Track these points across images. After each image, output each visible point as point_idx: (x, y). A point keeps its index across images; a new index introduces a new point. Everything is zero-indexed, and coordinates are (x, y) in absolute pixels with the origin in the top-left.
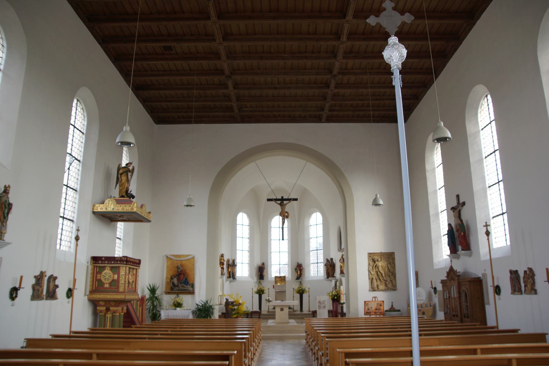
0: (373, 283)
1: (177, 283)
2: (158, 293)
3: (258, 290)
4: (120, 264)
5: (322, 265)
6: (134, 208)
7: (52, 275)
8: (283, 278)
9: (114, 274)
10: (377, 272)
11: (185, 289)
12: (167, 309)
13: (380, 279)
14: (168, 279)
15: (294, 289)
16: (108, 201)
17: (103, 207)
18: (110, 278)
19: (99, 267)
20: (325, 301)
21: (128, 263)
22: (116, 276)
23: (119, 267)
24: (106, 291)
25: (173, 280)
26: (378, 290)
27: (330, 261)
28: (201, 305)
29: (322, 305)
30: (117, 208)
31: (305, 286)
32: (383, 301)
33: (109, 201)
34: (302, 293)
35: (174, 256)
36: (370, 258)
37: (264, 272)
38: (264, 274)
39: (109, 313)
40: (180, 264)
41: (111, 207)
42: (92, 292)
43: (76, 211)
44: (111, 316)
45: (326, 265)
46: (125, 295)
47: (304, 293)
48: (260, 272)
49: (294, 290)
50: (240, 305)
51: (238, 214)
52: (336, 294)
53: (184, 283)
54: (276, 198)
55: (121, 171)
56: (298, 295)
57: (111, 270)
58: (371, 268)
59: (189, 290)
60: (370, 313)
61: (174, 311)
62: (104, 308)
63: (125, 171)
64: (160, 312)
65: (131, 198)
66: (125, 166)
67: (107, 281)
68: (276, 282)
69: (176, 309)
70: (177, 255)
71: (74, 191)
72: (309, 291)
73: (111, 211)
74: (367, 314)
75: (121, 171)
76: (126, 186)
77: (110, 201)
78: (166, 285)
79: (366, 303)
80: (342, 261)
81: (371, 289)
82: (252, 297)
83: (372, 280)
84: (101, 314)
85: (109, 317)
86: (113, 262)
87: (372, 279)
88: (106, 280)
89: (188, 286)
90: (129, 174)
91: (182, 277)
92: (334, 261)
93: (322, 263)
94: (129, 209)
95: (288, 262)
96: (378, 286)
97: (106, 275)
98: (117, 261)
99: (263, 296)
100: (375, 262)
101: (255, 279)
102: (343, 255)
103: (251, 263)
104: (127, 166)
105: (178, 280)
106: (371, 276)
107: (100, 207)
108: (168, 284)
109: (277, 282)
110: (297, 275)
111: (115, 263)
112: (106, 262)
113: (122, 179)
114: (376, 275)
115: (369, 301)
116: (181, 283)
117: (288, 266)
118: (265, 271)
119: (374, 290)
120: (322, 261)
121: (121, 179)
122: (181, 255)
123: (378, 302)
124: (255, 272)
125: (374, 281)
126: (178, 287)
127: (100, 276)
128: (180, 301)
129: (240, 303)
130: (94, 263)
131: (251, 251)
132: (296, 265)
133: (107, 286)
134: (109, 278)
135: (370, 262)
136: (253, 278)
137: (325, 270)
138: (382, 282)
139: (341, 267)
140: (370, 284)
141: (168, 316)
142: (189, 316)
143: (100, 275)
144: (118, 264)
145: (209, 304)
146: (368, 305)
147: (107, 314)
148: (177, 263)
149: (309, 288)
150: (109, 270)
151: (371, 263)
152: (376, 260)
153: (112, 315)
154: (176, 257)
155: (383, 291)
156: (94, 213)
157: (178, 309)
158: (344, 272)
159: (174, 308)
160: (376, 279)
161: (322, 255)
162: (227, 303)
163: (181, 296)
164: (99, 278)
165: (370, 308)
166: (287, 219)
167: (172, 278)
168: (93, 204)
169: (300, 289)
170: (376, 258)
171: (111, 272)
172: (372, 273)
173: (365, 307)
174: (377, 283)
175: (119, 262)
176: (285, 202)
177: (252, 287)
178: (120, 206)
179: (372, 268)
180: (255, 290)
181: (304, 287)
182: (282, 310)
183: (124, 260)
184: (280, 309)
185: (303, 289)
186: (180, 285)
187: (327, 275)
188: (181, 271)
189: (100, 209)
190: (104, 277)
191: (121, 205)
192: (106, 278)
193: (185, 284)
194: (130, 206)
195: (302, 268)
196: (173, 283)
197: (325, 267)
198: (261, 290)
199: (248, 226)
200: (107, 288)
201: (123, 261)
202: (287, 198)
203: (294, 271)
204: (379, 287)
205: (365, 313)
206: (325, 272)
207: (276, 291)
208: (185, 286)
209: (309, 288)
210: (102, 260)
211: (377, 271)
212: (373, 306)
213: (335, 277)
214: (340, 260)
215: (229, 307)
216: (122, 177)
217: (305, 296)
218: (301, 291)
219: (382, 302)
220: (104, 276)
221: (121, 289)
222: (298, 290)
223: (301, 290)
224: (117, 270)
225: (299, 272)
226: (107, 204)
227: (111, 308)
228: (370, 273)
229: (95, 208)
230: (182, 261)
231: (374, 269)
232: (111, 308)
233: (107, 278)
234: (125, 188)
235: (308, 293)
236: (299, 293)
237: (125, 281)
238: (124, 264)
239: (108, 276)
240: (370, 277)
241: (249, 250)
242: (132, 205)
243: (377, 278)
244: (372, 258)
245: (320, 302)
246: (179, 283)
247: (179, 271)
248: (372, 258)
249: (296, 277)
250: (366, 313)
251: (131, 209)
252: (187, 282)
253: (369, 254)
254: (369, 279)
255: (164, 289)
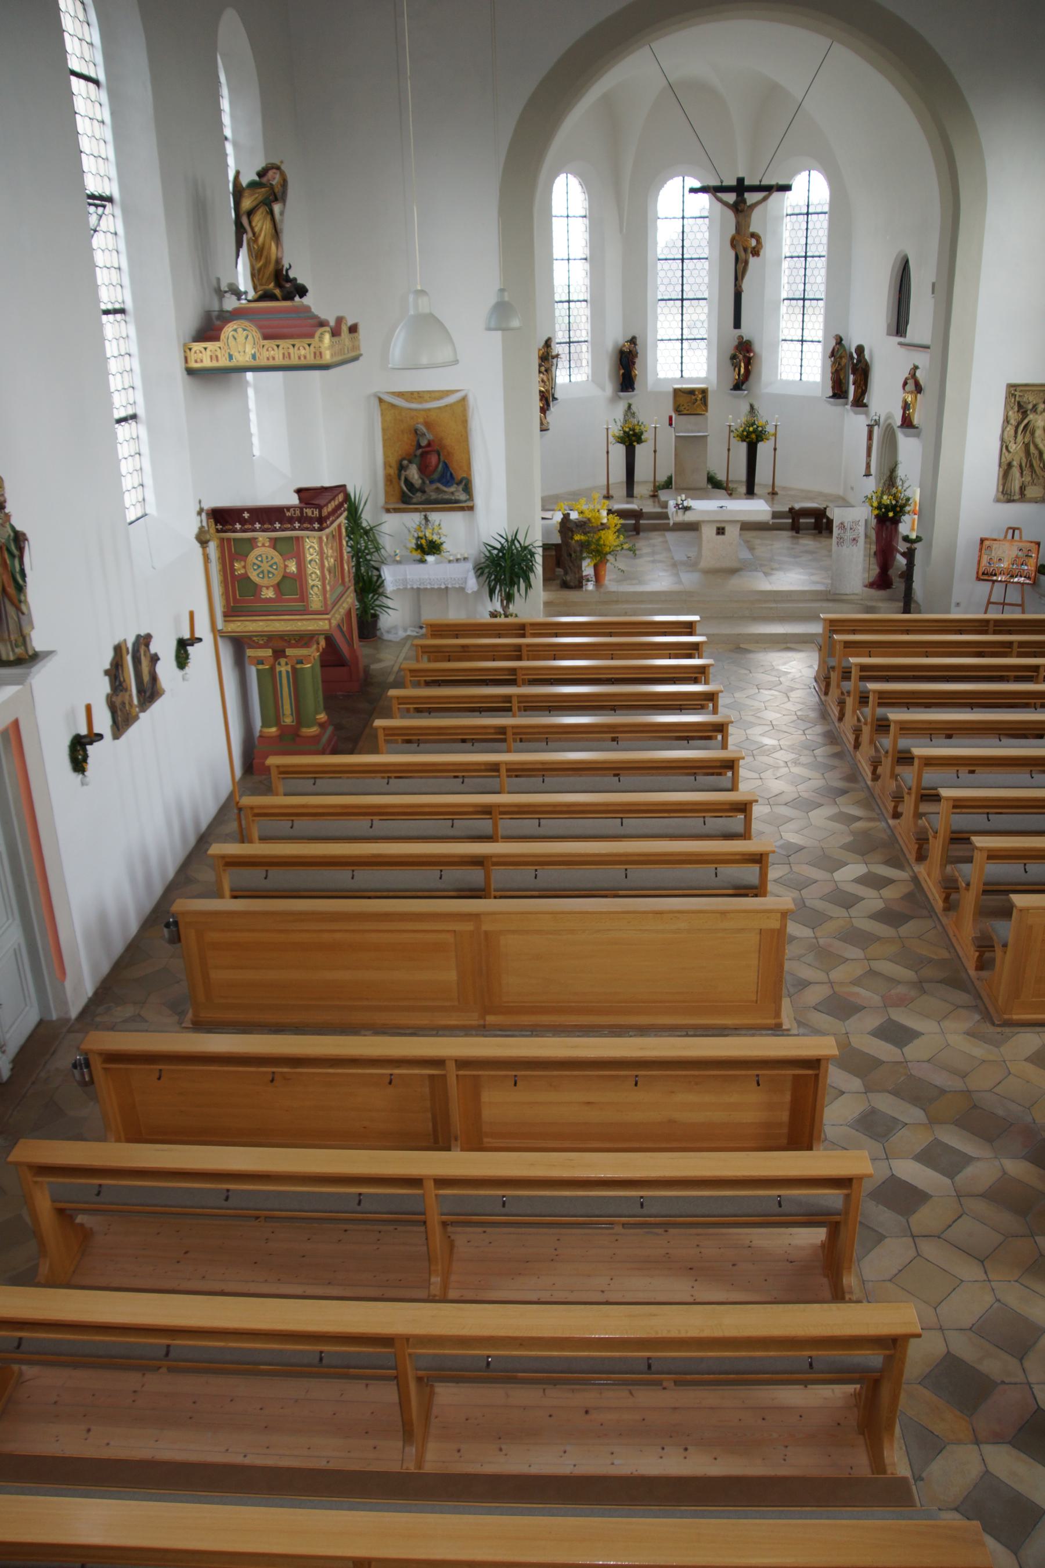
0: (1010, 478)
1: (420, 481)
2: (367, 518)
3: (625, 432)
4: (300, 529)
5: (819, 347)
6: (322, 350)
7: (138, 637)
8: (700, 396)
9: (285, 557)
10: (1027, 446)
11: (446, 497)
12: (399, 562)
13: (1031, 466)
14: (390, 467)
15: (732, 428)
16: (230, 329)
17: (219, 353)
18: (276, 569)
19: (234, 539)
20: (857, 523)
21: (325, 525)
22: (293, 568)
23: (297, 538)
24: (267, 611)
25: (407, 473)
26: (1023, 497)
27: (855, 356)
28: (499, 546)
29: (849, 535)
30: (265, 354)
31: (768, 418)
32: (1038, 544)
33: (235, 330)
34: (755, 440)
35: (400, 395)
36: (1013, 400)
37: (636, 366)
38: (637, 371)
39: (283, 661)
40: (421, 420)
41: (244, 352)
42: (230, 613)
43: (138, 383)
44: (290, 670)
45: (833, 354)
46: (329, 620)
47: (762, 440)
48: (623, 368)
49: (731, 431)
50: (602, 530)
51: (553, 182)
52: (894, 502)
53: (439, 480)
54: (719, 184)
55: (247, 204)
56: (743, 447)
57: (274, 548)
58: (1010, 430)
59: (457, 502)
60: (995, 575)
61: (421, 566)
62: (269, 652)
63: (261, 198)
64: (378, 569)
65: (297, 298)
66: (257, 178)
67: (266, 579)
68: (679, 406)
69: (422, 561)
70: (412, 393)
71: (119, 316)
72: (775, 435)
73: (247, 364)
74: (986, 577)
75: (247, 204)
76: (273, 257)
77: (240, 330)
78: (386, 485)
79: (986, 543)
80: (911, 386)
81: (1002, 497)
82: (608, 452)
83: (1006, 470)
84: (260, 667)
85: (284, 675)
86: (277, 525)
87: (1010, 465)
88: (263, 578)
89: (452, 489)
90: (277, 208)
91: (433, 459)
92: (867, 357)
93: (819, 342)
94: (308, 357)
95: (709, 331)
96: (1022, 489)
97: (262, 561)
98: (291, 520)
99: (639, 449)
100: (1025, 414)
101: (609, 388)
102: (916, 368)
103: (596, 341)
104: (264, 180)
105: (423, 470)
106: (1008, 457)
107: (209, 353)
108: (391, 481)
109: (682, 408)
110: (737, 377)
111: (285, 526)
112: (258, 526)
113: (257, 229)
114: (1023, 455)
115: (995, 540)
116: (431, 482)
117: (709, 346)
118: (638, 361)
119: (1009, 501)
120: (819, 335)
121: (254, 234)
122: (423, 392)
123: (1021, 545)
124: (607, 366)
125: (1015, 471)
126: (424, 492)
127: (244, 567)
128: (435, 538)
129: (602, 524)
130: (218, 531)
131: (596, 301)
132: (736, 343)
133: (270, 594)
134: (273, 571)
135: (1010, 413)
136: (603, 389)
137: (829, 370)
138: (1037, 475)
139: (906, 406)
140: (1001, 482)
141: (405, 581)
142: (465, 580)
143: (243, 563)
144: (294, 529)
145: (522, 543)
146: (992, 551)
147: (277, 663)
148: (412, 418)
149: (776, 426)
150: (269, 547)
151: (1014, 416)
152: (1030, 406)
153: (294, 669)
154: (407, 400)
155: (1036, 502)
156: (190, 372)
157: (430, 559)
158: (915, 422)
159: (417, 555)
160: (1021, 466)
161: (821, 318)
162: (566, 526)
163: (435, 517)
164: (243, 571)
165: (995, 560)
166: (755, 257)
167: (401, 468)
168: (182, 342)
169: (751, 429)
170: (1031, 399)
171: (276, 553)
172: (1013, 447)
173: (980, 556)
174: (1023, 479)
175: (297, 525)
176: (751, 198)
177: (608, 424)
178: (275, 348)
179: (1012, 432)
180: (616, 430)
181: (761, 422)
182: (721, 531)
183: (311, 518)
184: (714, 531)
185: (760, 429)
186: (430, 488)
187: (833, 388)
188: (429, 444)
189: (211, 357)
190: (255, 567)
191: (278, 342)
192: (262, 572)
193: (442, 484)
194: (309, 345)
195: (752, 355)
196: (407, 481)
197: (829, 362)
198: (635, 434)
199: (585, 217)
200: (269, 600)
201: (310, 520)
202: (758, 183)
203: (728, 362)
204: (1026, 492)
205: (980, 572)
206: (830, 375)
207: (677, 434)
208: (445, 489)
209: (776, 426)
210: (243, 522)
211: (1026, 440)
212: (1006, 554)
213: (865, 406)
214: (905, 384)
215: (572, 538)
216: (254, 224)
217: (763, 449)
218: (754, 436)
219: (1033, 545)
220: (254, 564)
221: (315, 601)
222: (745, 433)
223: (755, 431)
224: (293, 549)
225: (742, 365)
226: (231, 339)
227: (289, 652)
228: (1007, 447)
229: (192, 357)
230: (429, 410)
231: (1020, 437)
232: (289, 652)
233: (266, 572)
234: (270, 262)
235: (773, 438)
236: (748, 440)
237: (323, 578)
238: (314, 530)
239: (269, 564)
240: (1003, 459)
241: (589, 299)
242: (315, 341)
243: (1024, 465)
244: (1017, 399)
245: (842, 526)
246: (428, 482)
247: (424, 443)
248: (1017, 399)
249: (732, 387)
250: (983, 574)
251: (315, 354)
252: (449, 474)
253: (1011, 386)
254: (1000, 466)
255: (381, 500)
